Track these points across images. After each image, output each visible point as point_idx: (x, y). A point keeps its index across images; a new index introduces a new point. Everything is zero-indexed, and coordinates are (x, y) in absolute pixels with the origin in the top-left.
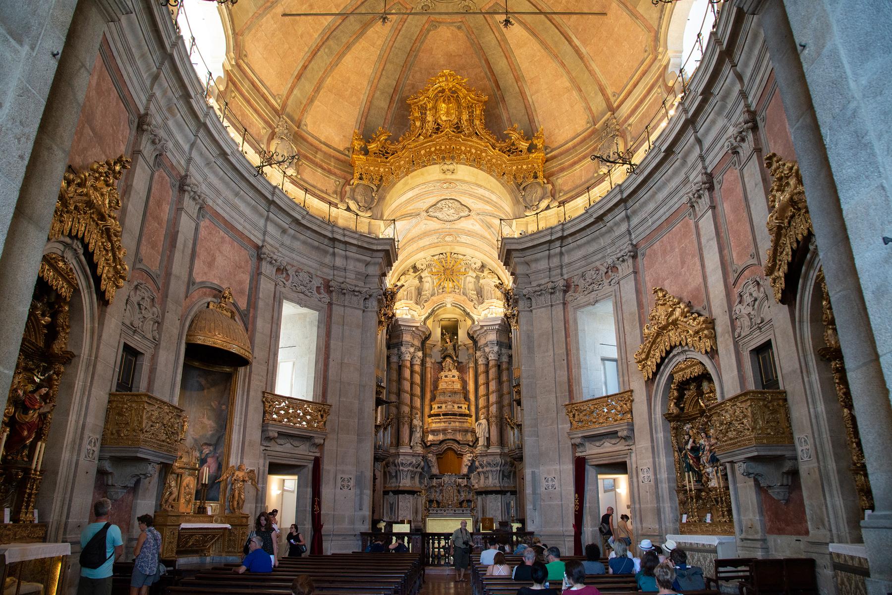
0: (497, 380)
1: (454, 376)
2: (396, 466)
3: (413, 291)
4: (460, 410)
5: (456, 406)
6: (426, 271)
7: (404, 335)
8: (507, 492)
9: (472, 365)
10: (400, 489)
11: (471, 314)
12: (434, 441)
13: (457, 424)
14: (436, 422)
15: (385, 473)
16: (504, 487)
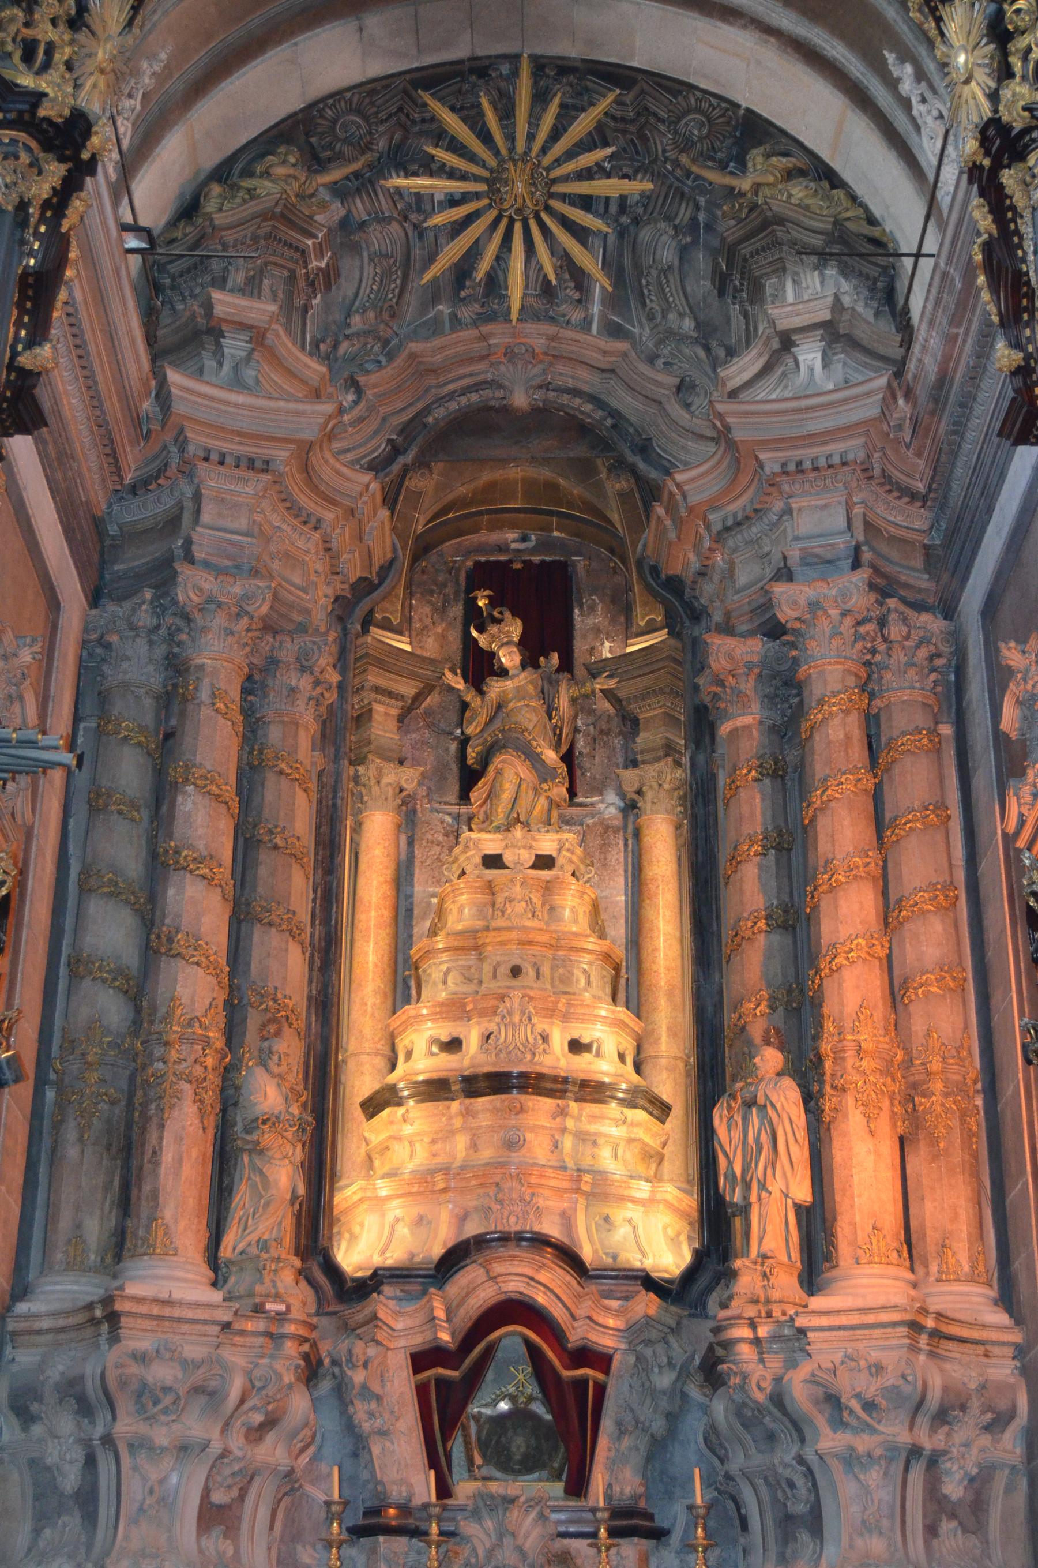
1: (544, 862)
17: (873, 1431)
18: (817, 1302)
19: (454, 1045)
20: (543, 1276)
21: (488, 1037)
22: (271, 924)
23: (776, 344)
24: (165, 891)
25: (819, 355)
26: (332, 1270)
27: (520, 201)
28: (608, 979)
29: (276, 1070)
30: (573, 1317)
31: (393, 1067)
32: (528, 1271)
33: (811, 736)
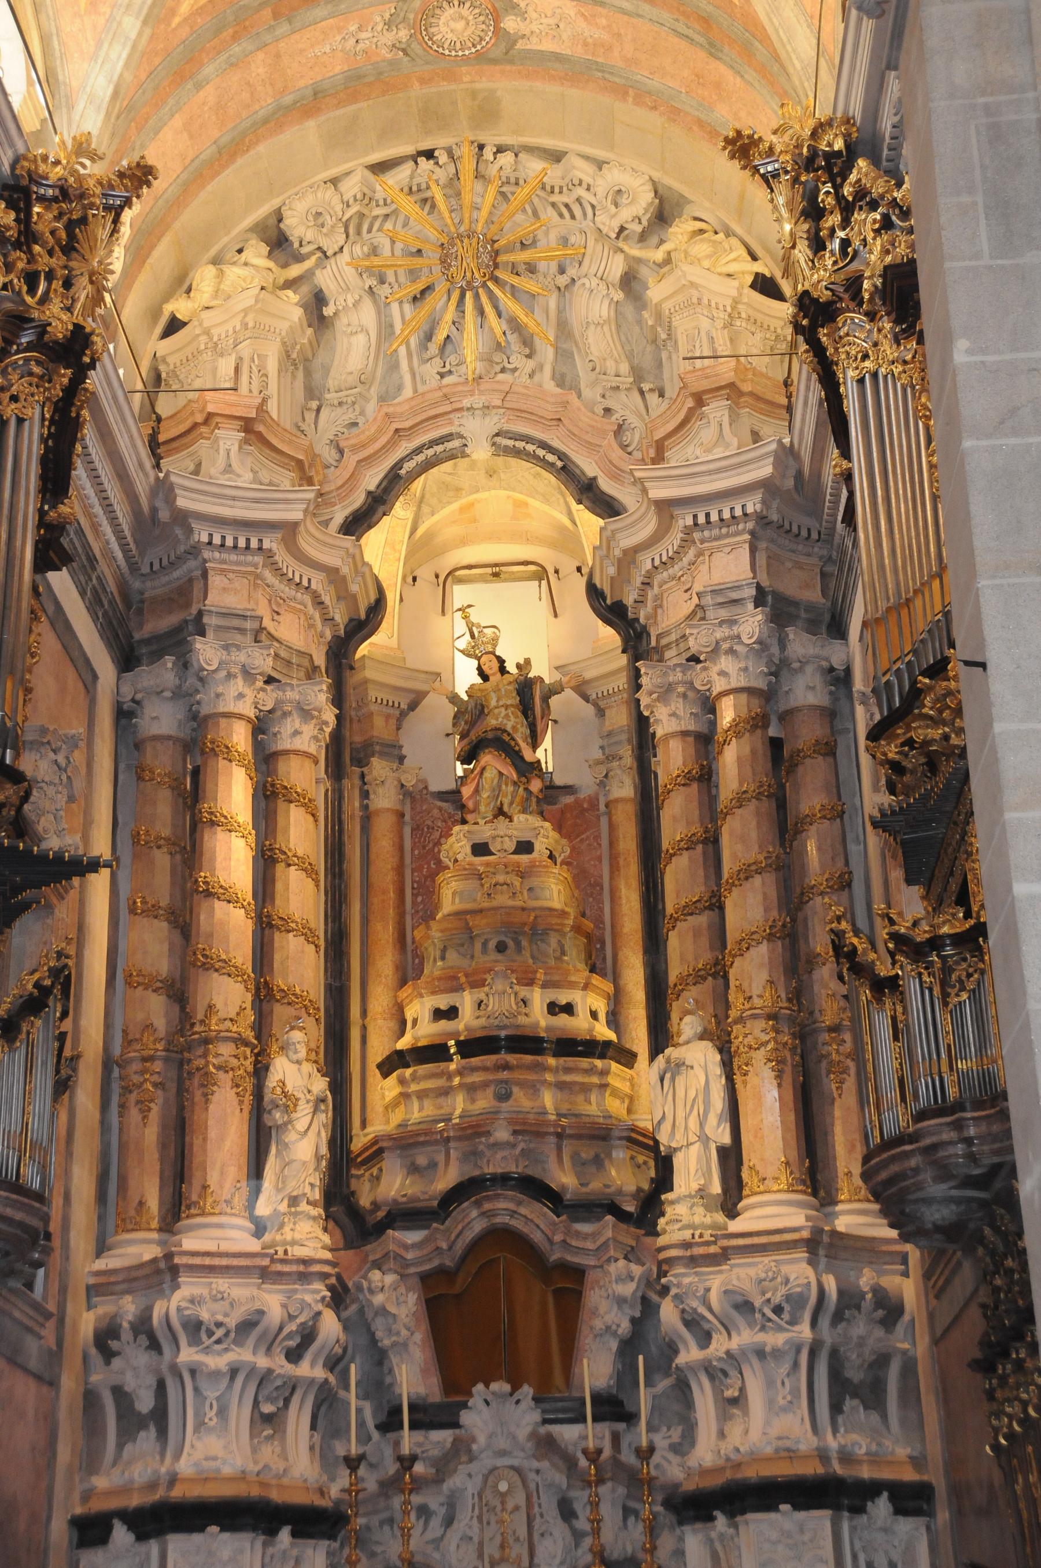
0: (768, 806)
1: (525, 847)
2: (155, 1345)
3: (272, 366)
4: (563, 1019)
5: (538, 999)
6: (346, 256)
7: (216, 581)
8: (871, 1490)
9: (624, 788)
10: (177, 1493)
11: (605, 485)
12: (414, 1199)
13: (548, 1099)
14: (421, 1095)
15: (90, 1399)
16: (846, 1457)
17: (781, 1329)
18: (735, 1226)
19: (451, 1013)
20: (523, 1210)
21: (479, 1005)
22: (289, 931)
23: (690, 403)
24: (199, 915)
25: (726, 412)
26: (355, 1213)
27: (469, 275)
28: (582, 947)
29: (295, 1057)
30: (550, 1241)
31: (402, 1033)
32: (511, 1206)
33: (720, 753)
